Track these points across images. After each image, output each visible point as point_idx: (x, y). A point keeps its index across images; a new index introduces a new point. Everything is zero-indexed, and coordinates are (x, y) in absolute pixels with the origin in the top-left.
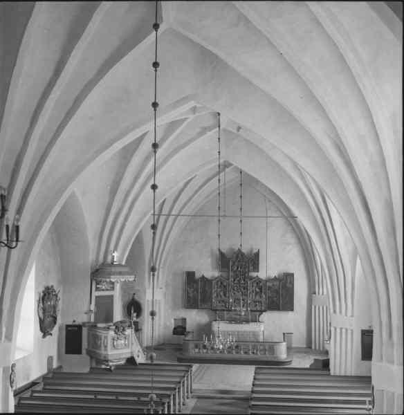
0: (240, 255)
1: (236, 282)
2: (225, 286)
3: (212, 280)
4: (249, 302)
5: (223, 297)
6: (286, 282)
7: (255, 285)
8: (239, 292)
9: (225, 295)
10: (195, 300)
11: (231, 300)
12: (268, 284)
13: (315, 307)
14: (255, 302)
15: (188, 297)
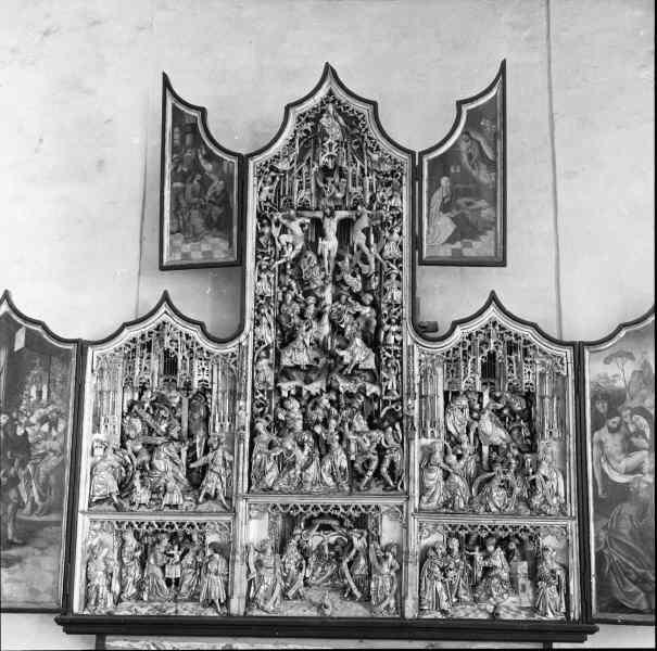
0: (332, 127)
1: (300, 356)
3: (82, 346)
8: (322, 447)
9: (196, 478)
12: (594, 369)
14: (473, 542)
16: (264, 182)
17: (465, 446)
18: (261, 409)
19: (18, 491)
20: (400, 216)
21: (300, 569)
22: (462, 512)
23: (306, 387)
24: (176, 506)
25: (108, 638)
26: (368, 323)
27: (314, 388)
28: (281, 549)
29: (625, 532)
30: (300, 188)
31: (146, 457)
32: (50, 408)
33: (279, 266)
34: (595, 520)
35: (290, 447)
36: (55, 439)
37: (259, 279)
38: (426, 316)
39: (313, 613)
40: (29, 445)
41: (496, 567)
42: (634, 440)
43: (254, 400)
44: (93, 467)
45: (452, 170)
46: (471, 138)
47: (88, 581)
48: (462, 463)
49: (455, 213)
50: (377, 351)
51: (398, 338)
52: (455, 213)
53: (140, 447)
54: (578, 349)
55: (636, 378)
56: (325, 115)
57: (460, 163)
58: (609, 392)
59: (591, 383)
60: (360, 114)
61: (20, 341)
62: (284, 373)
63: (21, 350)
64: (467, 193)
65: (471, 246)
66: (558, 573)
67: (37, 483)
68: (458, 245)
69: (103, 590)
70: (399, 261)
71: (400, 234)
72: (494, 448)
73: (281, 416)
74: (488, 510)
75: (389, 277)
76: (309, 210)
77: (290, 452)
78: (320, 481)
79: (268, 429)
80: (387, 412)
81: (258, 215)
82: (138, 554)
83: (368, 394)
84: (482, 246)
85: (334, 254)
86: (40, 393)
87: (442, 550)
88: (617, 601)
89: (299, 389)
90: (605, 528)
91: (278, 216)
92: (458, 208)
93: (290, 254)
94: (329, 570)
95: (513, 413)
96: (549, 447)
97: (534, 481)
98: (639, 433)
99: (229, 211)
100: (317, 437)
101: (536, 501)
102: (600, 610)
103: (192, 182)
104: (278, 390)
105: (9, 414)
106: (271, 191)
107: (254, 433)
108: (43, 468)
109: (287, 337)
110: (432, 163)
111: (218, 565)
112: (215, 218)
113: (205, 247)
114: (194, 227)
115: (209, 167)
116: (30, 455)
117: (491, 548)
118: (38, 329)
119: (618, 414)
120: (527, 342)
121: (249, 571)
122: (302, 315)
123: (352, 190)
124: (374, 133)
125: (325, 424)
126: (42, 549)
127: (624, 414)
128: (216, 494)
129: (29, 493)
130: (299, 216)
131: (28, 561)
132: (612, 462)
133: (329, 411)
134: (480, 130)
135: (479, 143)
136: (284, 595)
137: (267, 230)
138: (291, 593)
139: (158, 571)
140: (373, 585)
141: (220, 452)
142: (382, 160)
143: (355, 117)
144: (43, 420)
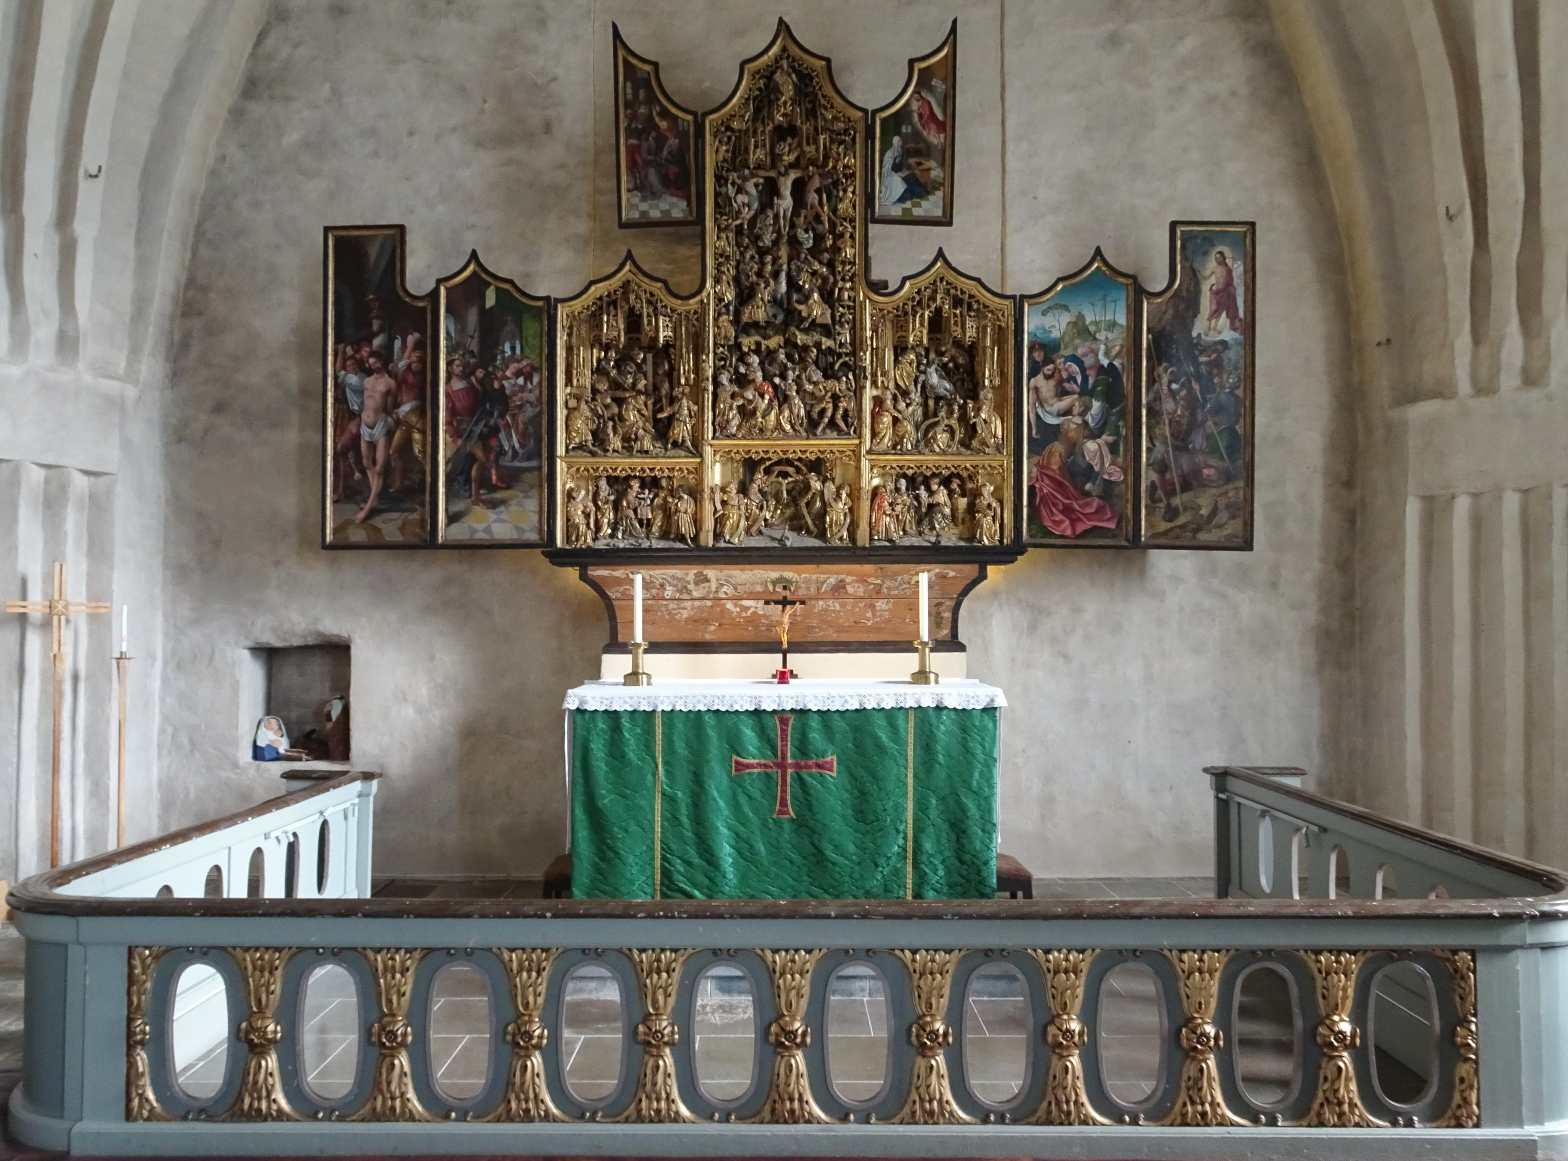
2: (665, 354)
3: (550, 304)
4: (870, 480)
5: (647, 444)
6: (1186, 302)
7: (918, 332)
9: (662, 430)
10: (408, 486)
11: (716, 474)
13: (1435, 511)
15: (350, 451)
16: (720, 142)
17: (913, 396)
18: (723, 363)
19: (500, 441)
20: (853, 175)
21: (761, 508)
22: (908, 453)
23: (763, 342)
24: (647, 452)
25: (590, 568)
26: (825, 280)
27: (774, 341)
28: (743, 490)
29: (1055, 467)
30: (756, 147)
31: (616, 410)
32: (524, 363)
33: (736, 226)
34: (1028, 458)
35: (751, 397)
36: (530, 391)
37: (719, 238)
38: (876, 274)
39: (776, 544)
40: (506, 396)
41: (938, 504)
42: (1066, 385)
43: (715, 353)
44: (568, 418)
45: (904, 129)
46: (924, 99)
47: (568, 520)
48: (910, 409)
49: (905, 173)
50: (832, 307)
51: (852, 294)
52: (905, 173)
53: (609, 401)
54: (1019, 301)
55: (1070, 327)
56: (779, 71)
57: (910, 122)
58: (1045, 342)
59: (1029, 333)
60: (813, 71)
61: (491, 299)
62: (744, 328)
63: (492, 308)
64: (917, 153)
65: (920, 206)
66: (994, 505)
67: (517, 433)
68: (908, 205)
69: (583, 528)
70: (852, 221)
71: (853, 193)
72: (938, 399)
73: (742, 370)
74: (932, 451)
75: (842, 235)
76: (764, 169)
77: (750, 402)
78: (779, 426)
79: (731, 381)
80: (842, 365)
81: (716, 176)
82: (612, 498)
83: (823, 347)
84: (932, 206)
85: (789, 214)
86: (513, 349)
87: (891, 486)
88: (1045, 527)
89: (758, 344)
90: (1037, 465)
91: (733, 176)
92: (909, 167)
93: (747, 214)
94: (789, 512)
95: (957, 366)
96: (987, 395)
97: (975, 424)
98: (1072, 379)
99: (686, 171)
100: (775, 387)
101: (975, 443)
102: (1031, 536)
103: (647, 139)
104: (738, 346)
105: (486, 369)
106: (727, 151)
107: (717, 383)
108: (521, 418)
109: (746, 295)
110: (884, 121)
111: (686, 505)
112: (672, 177)
113: (664, 206)
114: (651, 185)
115: (663, 124)
116: (507, 405)
117: (935, 487)
118: (506, 286)
119: (1053, 362)
120: (971, 296)
121: (716, 511)
122: (759, 274)
123: (807, 149)
124: (828, 90)
125: (783, 377)
126: (525, 492)
127: (1058, 361)
128: (684, 441)
129: (511, 441)
130: (756, 176)
131: (513, 502)
132: (1045, 405)
133: (785, 366)
134: (931, 89)
135: (929, 103)
136: (748, 531)
137: (723, 190)
138: (754, 530)
139: (631, 513)
140: (828, 519)
141: (685, 401)
142: (835, 118)
143: (809, 74)
144: (517, 374)
